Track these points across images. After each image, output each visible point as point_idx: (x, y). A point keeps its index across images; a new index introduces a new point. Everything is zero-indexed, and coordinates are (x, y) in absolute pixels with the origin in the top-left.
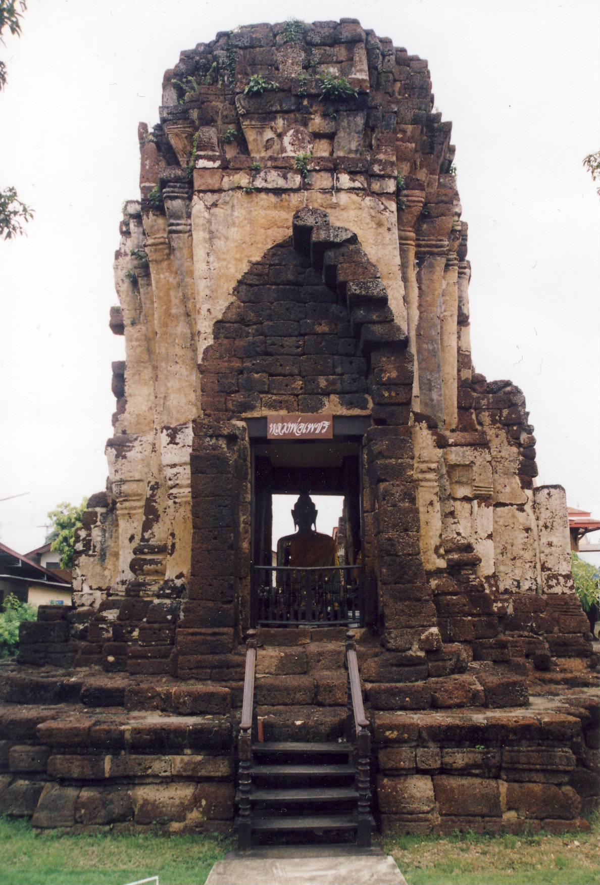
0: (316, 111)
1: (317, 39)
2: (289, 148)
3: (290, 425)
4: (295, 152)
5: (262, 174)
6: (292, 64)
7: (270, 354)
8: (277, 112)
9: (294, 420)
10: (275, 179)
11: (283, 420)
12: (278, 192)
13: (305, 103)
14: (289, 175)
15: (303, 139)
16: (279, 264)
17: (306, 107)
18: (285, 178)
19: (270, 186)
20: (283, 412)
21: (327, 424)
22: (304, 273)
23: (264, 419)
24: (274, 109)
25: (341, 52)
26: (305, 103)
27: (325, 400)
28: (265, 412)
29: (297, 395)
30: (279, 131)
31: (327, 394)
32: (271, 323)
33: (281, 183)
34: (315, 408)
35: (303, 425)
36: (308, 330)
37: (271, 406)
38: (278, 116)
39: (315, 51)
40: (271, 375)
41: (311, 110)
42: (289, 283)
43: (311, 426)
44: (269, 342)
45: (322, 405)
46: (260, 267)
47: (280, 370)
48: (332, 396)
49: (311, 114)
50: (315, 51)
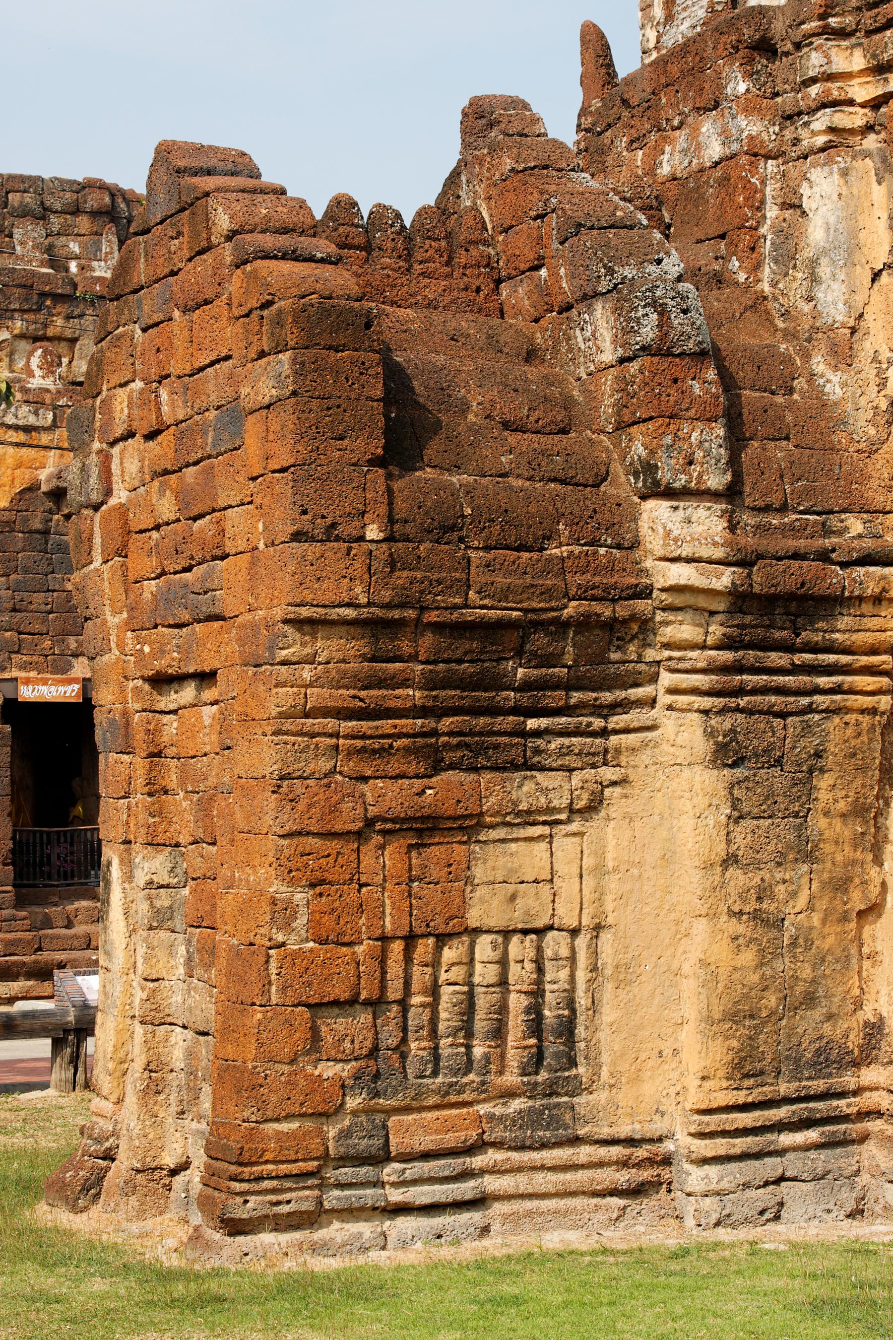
0: (59, 314)
1: (58, 206)
2: (38, 372)
3: (40, 687)
4: (43, 377)
5: (13, 409)
6: (33, 247)
7: (19, 611)
8: (15, 310)
9: (45, 682)
10: (25, 415)
11: (36, 682)
12: (27, 429)
13: (48, 303)
14: (41, 411)
15: (53, 361)
16: (27, 511)
17: (48, 307)
18: (36, 413)
19: (20, 423)
20: (33, 674)
21: (76, 687)
22: (51, 520)
23: (16, 679)
24: (12, 307)
25: (84, 223)
26: (48, 303)
27: (73, 660)
28: (15, 673)
29: (47, 656)
30: (17, 332)
31: (76, 655)
32: (20, 577)
33: (32, 420)
34: (65, 669)
35: (53, 688)
36: (57, 587)
37: (23, 667)
38: (16, 315)
39: (53, 218)
40: (20, 633)
41: (54, 311)
42: (37, 532)
43: (62, 689)
44: (18, 598)
45: (70, 666)
46: (8, 513)
47: (29, 629)
48: (81, 659)
49: (53, 315)
50: (53, 218)
